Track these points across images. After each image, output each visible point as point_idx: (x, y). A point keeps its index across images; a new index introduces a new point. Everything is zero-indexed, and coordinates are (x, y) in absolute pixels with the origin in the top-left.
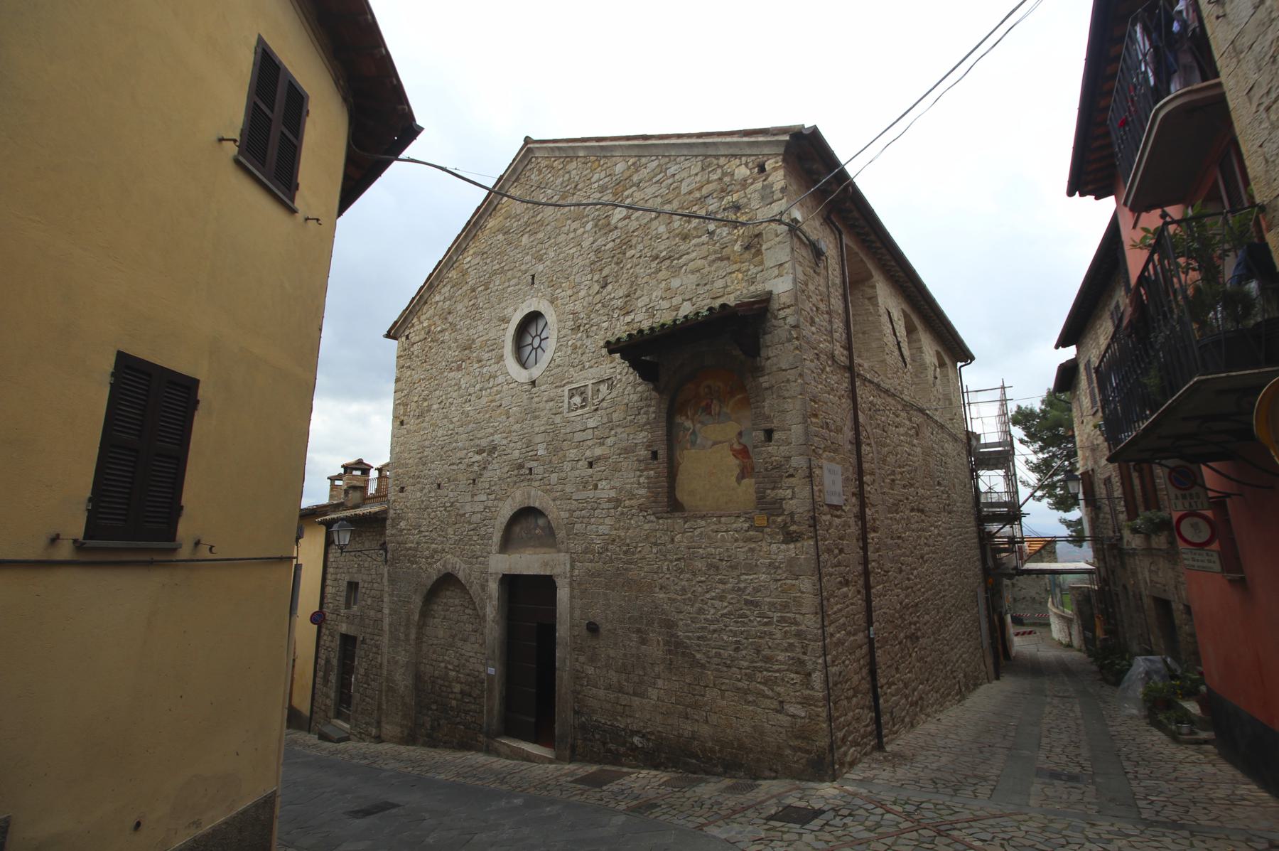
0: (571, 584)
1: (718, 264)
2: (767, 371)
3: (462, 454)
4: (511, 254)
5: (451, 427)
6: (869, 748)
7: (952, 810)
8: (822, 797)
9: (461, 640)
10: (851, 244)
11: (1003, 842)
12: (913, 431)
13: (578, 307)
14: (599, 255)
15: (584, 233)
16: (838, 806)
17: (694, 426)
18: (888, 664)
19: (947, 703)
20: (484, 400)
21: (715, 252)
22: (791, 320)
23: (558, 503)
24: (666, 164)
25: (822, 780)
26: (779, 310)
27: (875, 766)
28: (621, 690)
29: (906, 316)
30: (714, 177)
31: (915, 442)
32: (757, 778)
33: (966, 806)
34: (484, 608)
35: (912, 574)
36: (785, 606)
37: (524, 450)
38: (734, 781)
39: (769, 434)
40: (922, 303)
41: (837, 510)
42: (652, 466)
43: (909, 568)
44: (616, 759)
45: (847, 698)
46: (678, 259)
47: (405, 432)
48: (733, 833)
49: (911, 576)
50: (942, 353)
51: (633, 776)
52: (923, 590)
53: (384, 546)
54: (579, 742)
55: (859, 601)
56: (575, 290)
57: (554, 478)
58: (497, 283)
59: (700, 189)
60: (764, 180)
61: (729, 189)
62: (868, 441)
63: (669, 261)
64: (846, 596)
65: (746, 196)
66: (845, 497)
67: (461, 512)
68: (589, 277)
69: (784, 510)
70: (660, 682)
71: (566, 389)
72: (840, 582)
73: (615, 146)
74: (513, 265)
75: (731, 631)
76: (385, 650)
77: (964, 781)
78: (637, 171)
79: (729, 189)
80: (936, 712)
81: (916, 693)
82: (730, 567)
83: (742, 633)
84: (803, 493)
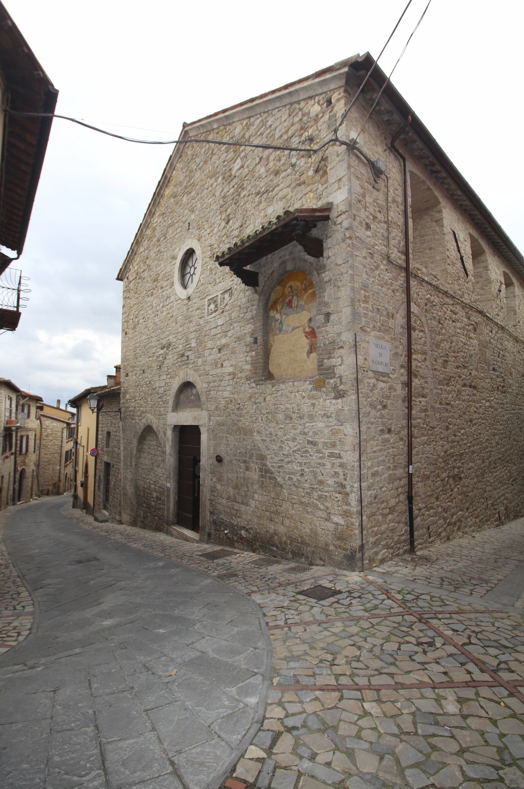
0: (208, 431)
1: (299, 188)
2: (328, 268)
3: (154, 350)
4: (178, 211)
5: (149, 333)
6: (401, 551)
7: (444, 602)
8: (347, 582)
9: (157, 466)
10: (417, 172)
11: (471, 634)
12: (471, 327)
13: (213, 241)
14: (225, 200)
15: (217, 186)
16: (354, 589)
17: (281, 317)
18: (428, 494)
19: (486, 526)
20: (165, 313)
21: (296, 180)
22: (345, 224)
23: (202, 378)
24: (266, 118)
25: (353, 571)
26: (337, 217)
27: (401, 564)
28: (235, 501)
29: (473, 241)
30: (297, 119)
31: (472, 335)
32: (312, 564)
33: (457, 601)
34: (165, 447)
35: (460, 432)
36: (334, 445)
37: (184, 345)
38: (297, 564)
39: (328, 315)
40: (489, 230)
41: (384, 377)
42: (254, 348)
43: (456, 427)
44: (230, 542)
45: (382, 514)
46: (272, 191)
47: (127, 339)
48: (267, 600)
49: (457, 433)
50: (510, 275)
51: (238, 555)
52: (469, 445)
53: (120, 411)
54: (213, 531)
55: (402, 446)
56: (211, 229)
57: (200, 361)
58: (170, 233)
59: (286, 132)
60: (331, 112)
61: (306, 126)
62: (422, 329)
63: (266, 194)
64: (387, 441)
65: (317, 129)
66: (392, 368)
67: (154, 387)
68: (219, 217)
69: (335, 374)
70: (256, 496)
71: (206, 300)
72: (382, 431)
73: (234, 113)
74: (178, 218)
75: (298, 462)
76: (122, 471)
77: (468, 581)
78: (248, 129)
79: (306, 126)
80: (473, 531)
81: (454, 517)
82: (299, 417)
83: (305, 464)
84: (350, 360)
